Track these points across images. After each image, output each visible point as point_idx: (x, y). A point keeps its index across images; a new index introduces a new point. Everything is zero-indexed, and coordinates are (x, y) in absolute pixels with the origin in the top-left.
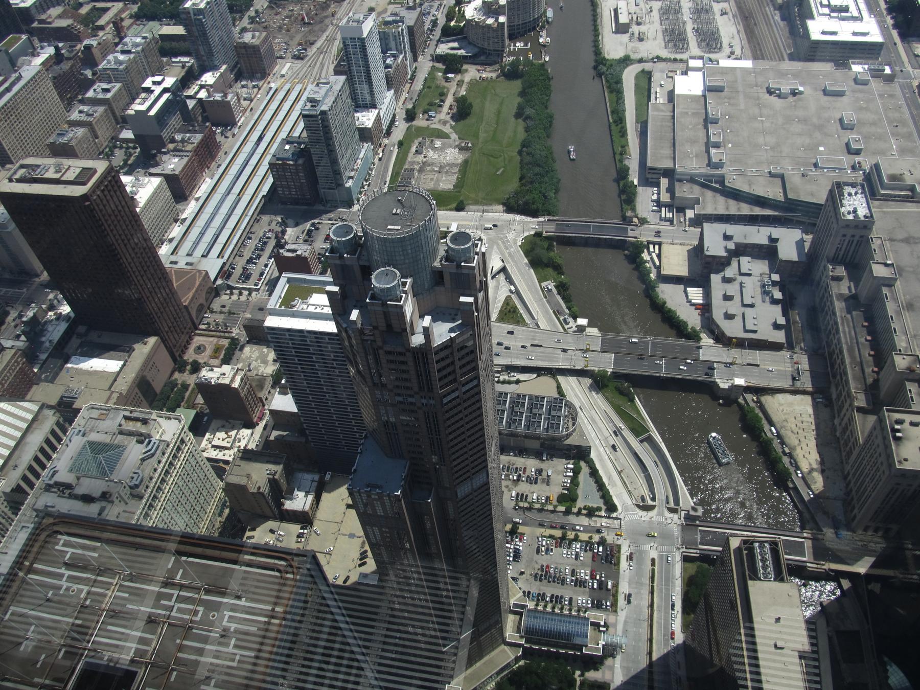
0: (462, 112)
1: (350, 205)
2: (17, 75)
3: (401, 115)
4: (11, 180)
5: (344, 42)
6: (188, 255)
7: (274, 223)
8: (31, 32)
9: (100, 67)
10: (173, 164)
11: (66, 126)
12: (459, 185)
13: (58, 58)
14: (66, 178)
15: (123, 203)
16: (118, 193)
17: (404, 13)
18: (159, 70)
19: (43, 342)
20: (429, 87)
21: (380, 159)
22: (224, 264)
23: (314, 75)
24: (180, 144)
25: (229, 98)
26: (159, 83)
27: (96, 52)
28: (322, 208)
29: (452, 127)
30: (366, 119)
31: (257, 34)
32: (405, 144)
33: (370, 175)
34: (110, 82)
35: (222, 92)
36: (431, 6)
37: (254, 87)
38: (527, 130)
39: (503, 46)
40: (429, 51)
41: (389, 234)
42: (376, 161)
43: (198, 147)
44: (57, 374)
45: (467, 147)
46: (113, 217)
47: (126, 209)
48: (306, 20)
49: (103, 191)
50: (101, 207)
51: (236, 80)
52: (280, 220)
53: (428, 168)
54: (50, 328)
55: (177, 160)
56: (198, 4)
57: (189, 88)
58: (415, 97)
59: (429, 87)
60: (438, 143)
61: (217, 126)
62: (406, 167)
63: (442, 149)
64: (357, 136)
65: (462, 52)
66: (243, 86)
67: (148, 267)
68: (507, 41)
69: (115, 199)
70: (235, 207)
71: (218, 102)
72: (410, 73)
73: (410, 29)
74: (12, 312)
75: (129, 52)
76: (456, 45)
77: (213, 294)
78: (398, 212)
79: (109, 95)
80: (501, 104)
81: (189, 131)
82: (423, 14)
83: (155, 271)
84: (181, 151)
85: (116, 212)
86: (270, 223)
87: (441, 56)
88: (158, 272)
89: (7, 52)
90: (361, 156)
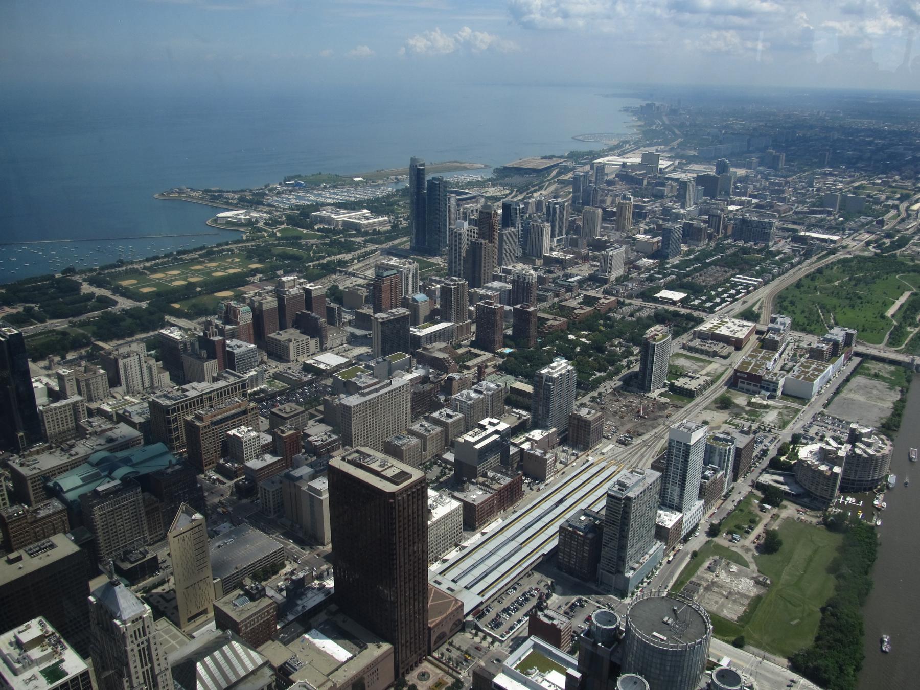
0: (770, 545)
1: (623, 594)
3: (704, 527)
4: (343, 459)
5: (670, 443)
6: (453, 580)
7: (543, 584)
8: (414, 355)
10: (476, 495)
11: (405, 433)
12: (745, 619)
13: (424, 380)
14: (383, 473)
15: (420, 512)
16: (420, 502)
17: (736, 434)
18: (499, 414)
19: (297, 605)
20: (741, 510)
21: (669, 562)
22: (482, 603)
23: (632, 462)
24: (489, 481)
25: (547, 457)
27: (455, 383)
28: (594, 587)
29: (754, 557)
30: (668, 519)
31: (593, 412)
32: (699, 557)
33: (653, 573)
34: (455, 410)
35: (544, 449)
36: (765, 437)
37: (573, 455)
38: (838, 588)
39: (832, 496)
40: (751, 477)
41: (652, 641)
42: (664, 562)
44: (293, 640)
45: (765, 583)
46: (406, 521)
47: (420, 518)
49: (409, 495)
50: (401, 508)
52: (550, 583)
53: (716, 589)
54: (309, 595)
55: (481, 493)
56: (553, 373)
58: (724, 515)
59: (741, 510)
60: (734, 568)
62: (693, 579)
63: (737, 575)
64: (653, 532)
65: (785, 488)
66: (564, 451)
67: (415, 577)
68: (837, 493)
69: (415, 506)
70: (513, 554)
71: (537, 456)
72: (726, 490)
73: (738, 451)
74: (288, 566)
75: (481, 393)
76: (781, 479)
77: (459, 627)
78: (670, 621)
79: (450, 421)
80: (815, 552)
81: (502, 473)
82: (754, 441)
83: (419, 583)
84: (488, 486)
85: (411, 518)
86: (539, 582)
87: (763, 484)
88: (421, 585)
89: (390, 362)
90: (651, 552)
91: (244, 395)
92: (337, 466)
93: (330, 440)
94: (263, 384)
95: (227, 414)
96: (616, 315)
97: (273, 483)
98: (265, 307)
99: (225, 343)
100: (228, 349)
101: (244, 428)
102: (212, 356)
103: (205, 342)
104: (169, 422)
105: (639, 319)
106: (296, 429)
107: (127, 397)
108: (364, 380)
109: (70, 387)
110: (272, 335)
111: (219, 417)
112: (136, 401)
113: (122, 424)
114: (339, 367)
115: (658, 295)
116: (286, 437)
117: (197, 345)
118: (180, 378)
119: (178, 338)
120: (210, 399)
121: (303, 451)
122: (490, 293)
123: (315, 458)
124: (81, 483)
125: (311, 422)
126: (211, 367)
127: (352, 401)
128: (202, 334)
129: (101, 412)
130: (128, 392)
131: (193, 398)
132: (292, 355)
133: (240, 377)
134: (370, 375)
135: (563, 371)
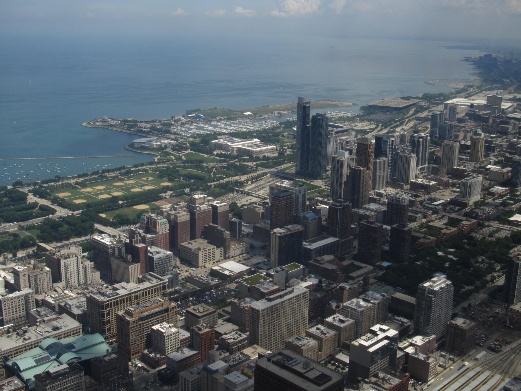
2: (291, 289)
8: (306, 265)
9: (344, 304)
11: (304, 334)
24: (381, 381)
25: (430, 361)
26: (384, 331)
27: (346, 293)
31: (468, 322)
34: (346, 316)
35: (426, 354)
43: (394, 388)
48: (508, 323)
51: (438, 349)
57: (401, 342)
61: (412, 377)
66: (442, 356)
71: (420, 360)
75: (368, 301)
79: (342, 325)
81: (391, 374)
89: (287, 271)
91: (164, 295)
92: (265, 367)
93: (240, 338)
94: (177, 285)
95: (152, 311)
96: (478, 236)
97: (192, 373)
98: (180, 220)
99: (147, 249)
100: (149, 254)
101: (165, 324)
102: (136, 259)
103: (130, 248)
104: (103, 316)
105: (499, 239)
106: (212, 327)
107: (66, 292)
108: (266, 287)
109: (23, 281)
110: (184, 244)
111: (146, 314)
112: (74, 295)
113: (65, 315)
114: (241, 274)
115: (512, 219)
116: (203, 334)
117: (123, 250)
118: (110, 278)
119: (108, 243)
120: (137, 297)
121: (217, 346)
122: (368, 213)
123: (227, 354)
124: (34, 364)
125: (220, 321)
126: (135, 269)
127: (260, 305)
128: (128, 241)
129: (44, 303)
130: (67, 287)
131: (123, 296)
132: (201, 262)
133: (161, 280)
134: (270, 282)
135: (443, 285)
